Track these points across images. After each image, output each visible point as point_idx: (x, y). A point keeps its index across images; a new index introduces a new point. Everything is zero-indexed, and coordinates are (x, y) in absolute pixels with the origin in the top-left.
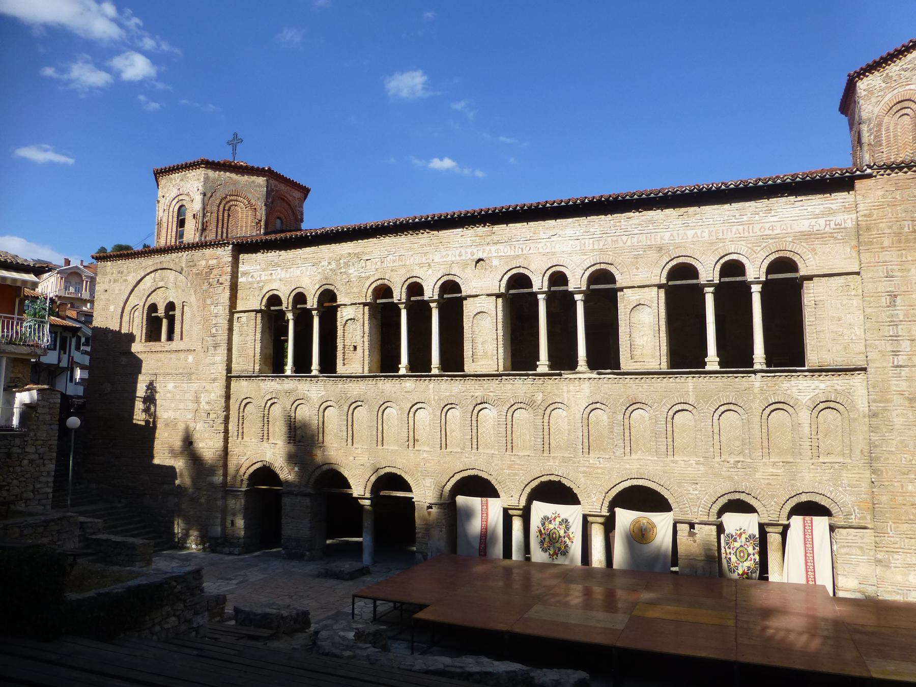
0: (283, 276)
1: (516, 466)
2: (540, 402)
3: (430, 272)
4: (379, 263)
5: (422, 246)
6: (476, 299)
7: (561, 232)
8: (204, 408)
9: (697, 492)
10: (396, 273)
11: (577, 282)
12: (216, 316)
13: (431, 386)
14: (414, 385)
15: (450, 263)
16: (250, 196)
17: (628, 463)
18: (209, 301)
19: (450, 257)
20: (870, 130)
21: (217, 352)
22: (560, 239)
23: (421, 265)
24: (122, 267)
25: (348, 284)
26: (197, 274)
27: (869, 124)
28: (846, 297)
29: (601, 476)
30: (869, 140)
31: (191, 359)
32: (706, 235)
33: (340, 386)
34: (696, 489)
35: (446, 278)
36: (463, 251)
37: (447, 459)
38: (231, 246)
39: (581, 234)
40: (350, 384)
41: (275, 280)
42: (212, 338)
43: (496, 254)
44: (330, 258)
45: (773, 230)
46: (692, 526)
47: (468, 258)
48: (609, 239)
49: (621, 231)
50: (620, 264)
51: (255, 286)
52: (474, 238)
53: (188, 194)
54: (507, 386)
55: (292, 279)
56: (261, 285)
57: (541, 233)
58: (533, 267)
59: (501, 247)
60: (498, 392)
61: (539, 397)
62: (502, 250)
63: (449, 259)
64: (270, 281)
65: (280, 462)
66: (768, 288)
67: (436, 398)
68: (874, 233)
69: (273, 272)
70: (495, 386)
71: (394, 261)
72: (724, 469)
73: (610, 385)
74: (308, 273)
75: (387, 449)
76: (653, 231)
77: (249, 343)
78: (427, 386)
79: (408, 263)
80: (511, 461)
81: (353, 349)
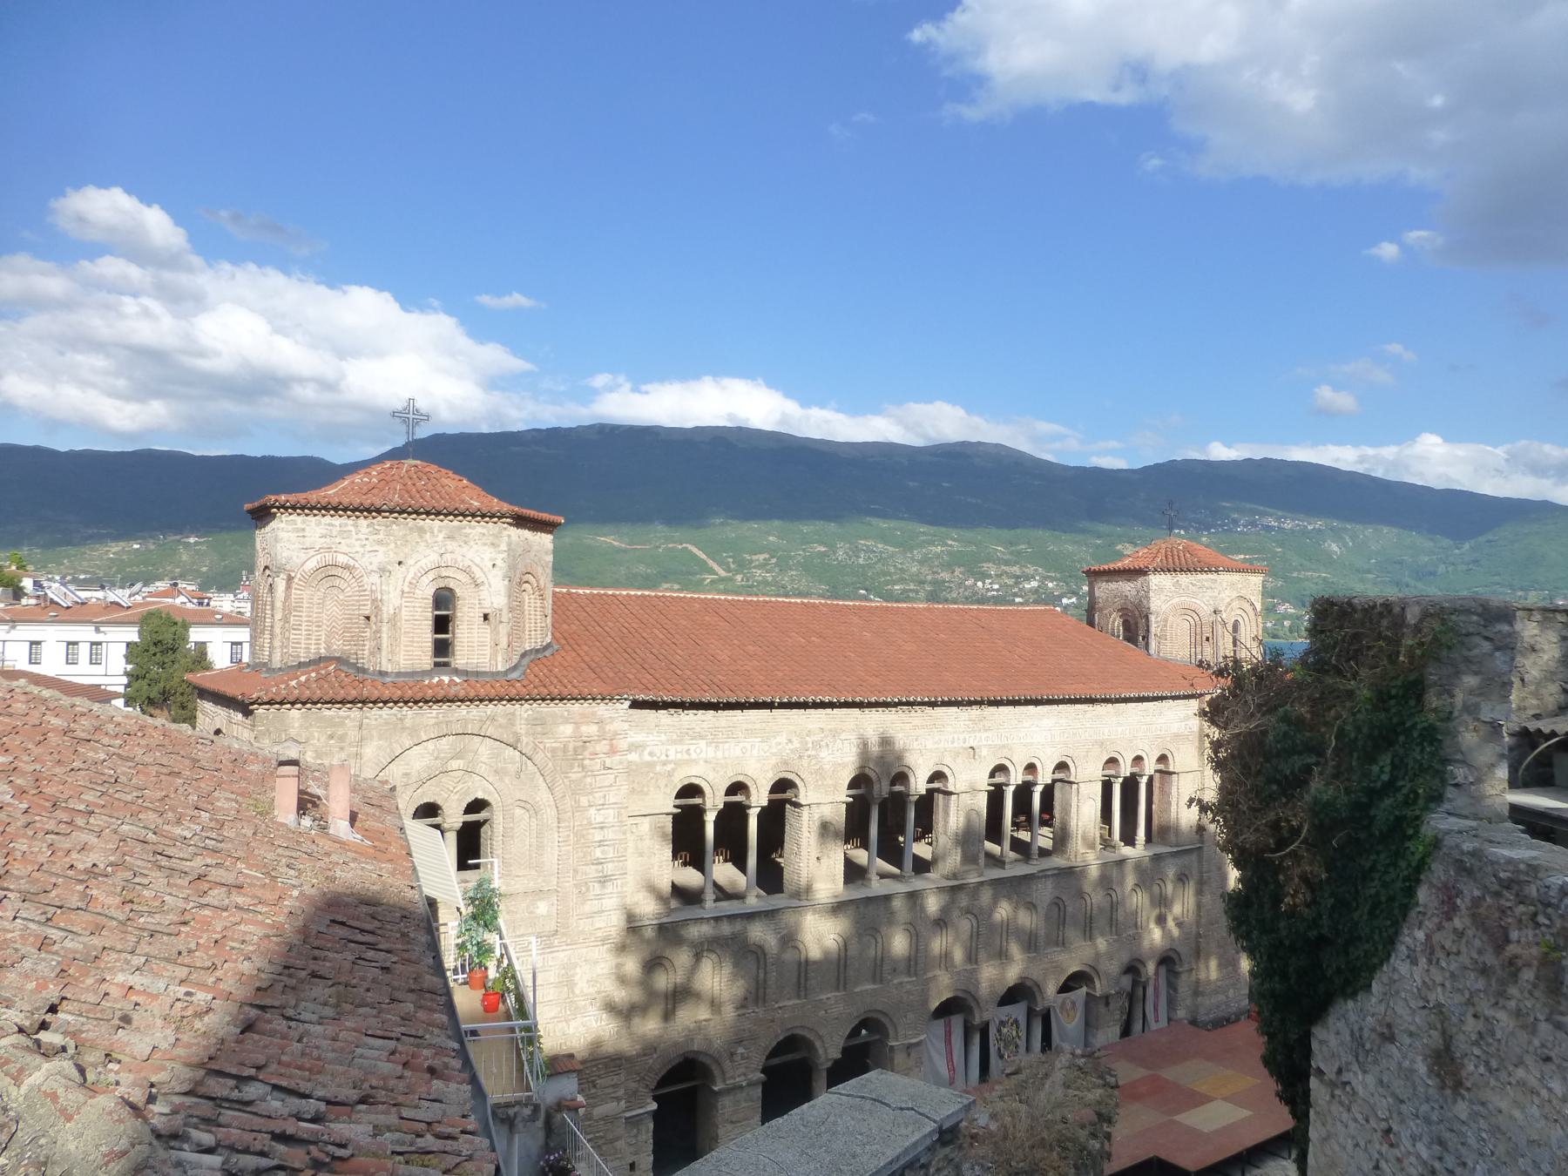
0: (710, 752)
5: (915, 727)
8: (582, 991)
12: (602, 828)
16: (540, 570)
18: (584, 801)
20: (1157, 622)
21: (606, 891)
24: (342, 724)
26: (554, 750)
31: (542, 908)
38: (628, 703)
41: (696, 761)
42: (594, 867)
52: (967, 723)
53: (466, 571)
56: (669, 767)
59: (989, 734)
66: (1151, 778)
69: (692, 748)
74: (755, 752)
77: (656, 868)
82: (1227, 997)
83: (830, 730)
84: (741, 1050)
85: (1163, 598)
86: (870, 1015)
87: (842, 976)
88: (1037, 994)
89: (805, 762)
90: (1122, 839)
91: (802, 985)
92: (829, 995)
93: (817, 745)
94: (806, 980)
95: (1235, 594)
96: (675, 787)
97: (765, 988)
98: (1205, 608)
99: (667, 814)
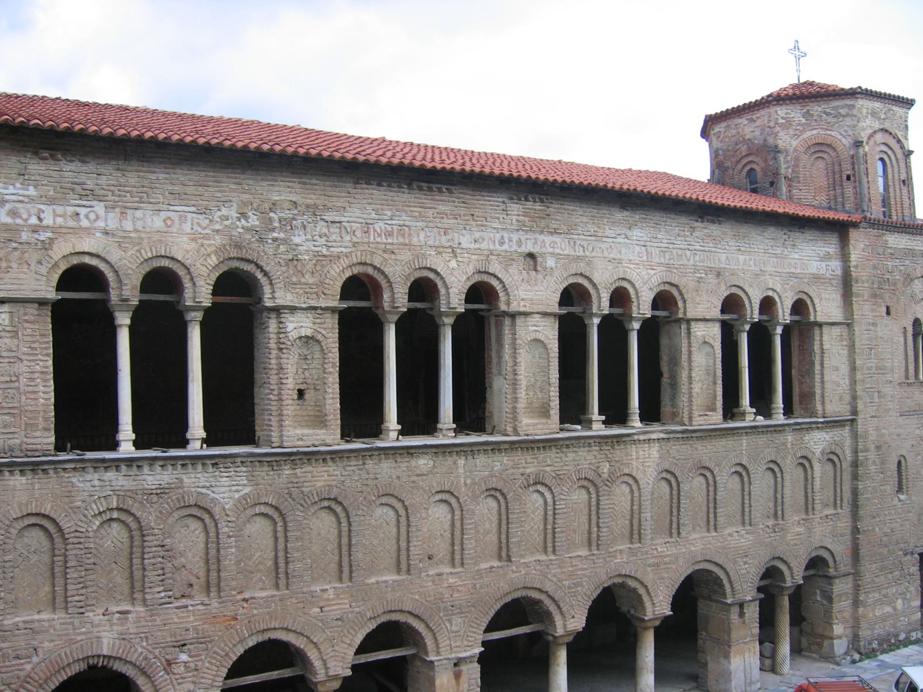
1: (579, 573)
2: (607, 475)
3: (453, 264)
4: (358, 233)
5: (442, 215)
6: (528, 319)
7: (629, 233)
9: (747, 566)
10: (393, 257)
11: (642, 308)
13: (461, 462)
14: (432, 463)
15: (486, 253)
17: (693, 544)
19: (485, 242)
22: (626, 240)
23: (441, 250)
25: (291, 267)
27: (787, 156)
28: (840, 347)
29: (669, 566)
30: (786, 172)
32: (752, 263)
33: (287, 472)
34: (746, 563)
35: (477, 278)
36: (506, 235)
37: (486, 579)
39: (649, 239)
40: (310, 468)
41: (88, 231)
43: (551, 250)
44: (244, 204)
45: (796, 268)
46: (741, 606)
47: (513, 249)
48: (674, 251)
49: (685, 243)
50: (685, 287)
51: (25, 236)
54: (569, 455)
55: (143, 235)
56: (44, 236)
57: (607, 228)
58: (596, 278)
59: (557, 239)
60: (557, 464)
61: (605, 468)
62: (559, 245)
63: (484, 246)
64: (77, 231)
65: (140, 650)
66: (787, 329)
67: (469, 482)
68: (859, 285)
69: (83, 211)
70: (553, 455)
71: (389, 234)
72: (767, 535)
73: (678, 447)
74: (187, 227)
75: (385, 582)
76: (713, 249)
77: (23, 380)
78: (455, 463)
79: (415, 240)
80: (572, 566)
81: (296, 397)
82: (895, 609)
83: (308, 206)
84: (184, 657)
85: (792, 132)
86: (394, 617)
87: (345, 560)
88: (645, 598)
89: (269, 249)
90: (751, 406)
91: (282, 570)
92: (327, 587)
93: (287, 224)
94: (287, 563)
95: (877, 126)
96: (56, 265)
97: (219, 571)
98: (844, 140)
99: (41, 303)
